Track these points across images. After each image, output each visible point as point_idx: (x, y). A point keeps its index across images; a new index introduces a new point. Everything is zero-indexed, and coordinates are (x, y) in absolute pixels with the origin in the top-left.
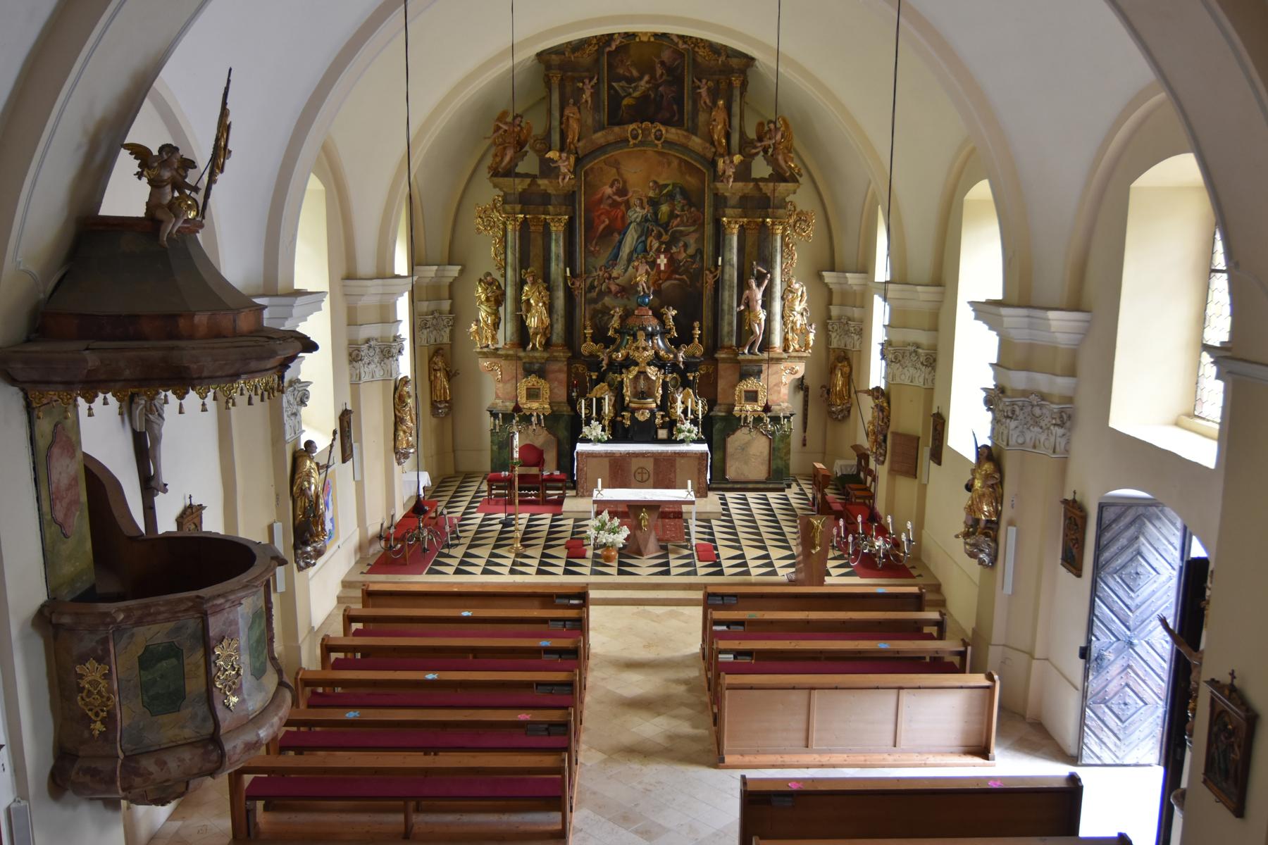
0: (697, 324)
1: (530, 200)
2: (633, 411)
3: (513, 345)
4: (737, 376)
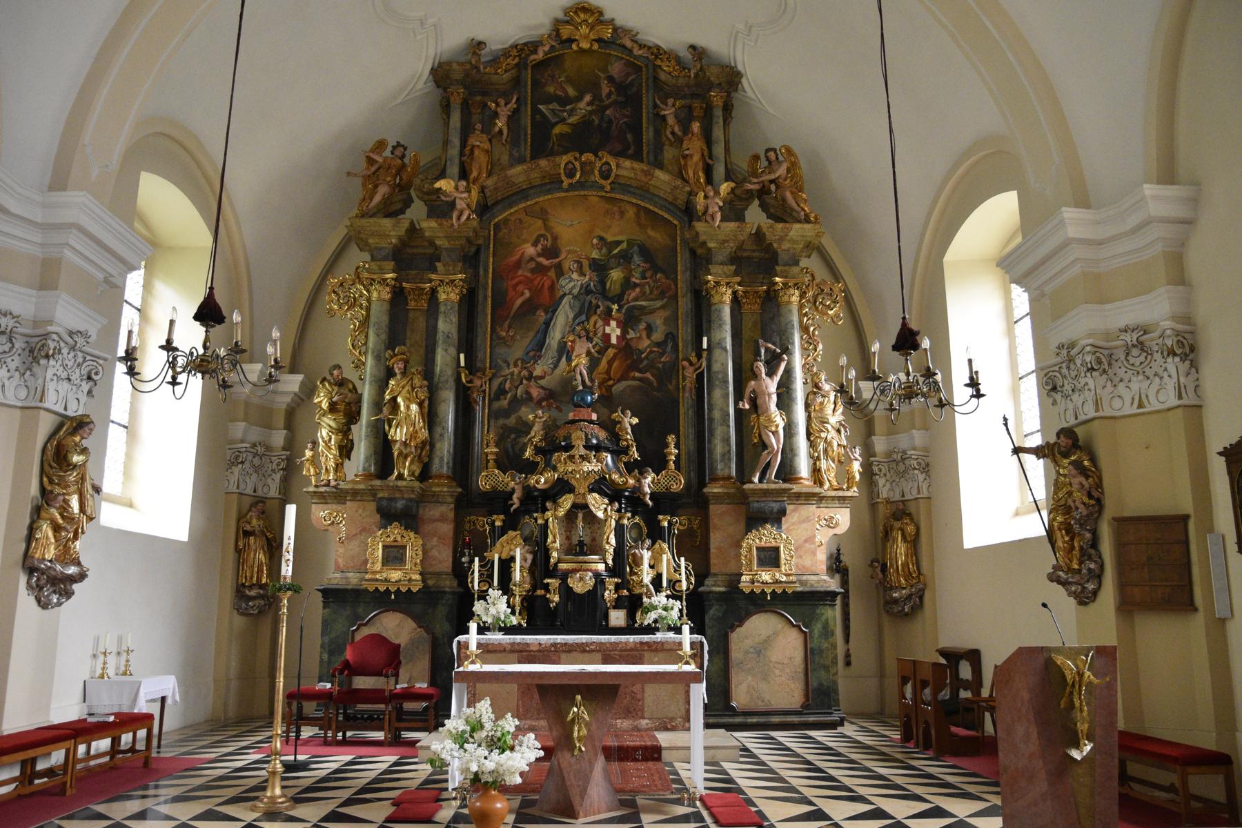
0: (671, 439)
1: (410, 257)
2: (564, 576)
3: (368, 476)
4: (742, 526)
